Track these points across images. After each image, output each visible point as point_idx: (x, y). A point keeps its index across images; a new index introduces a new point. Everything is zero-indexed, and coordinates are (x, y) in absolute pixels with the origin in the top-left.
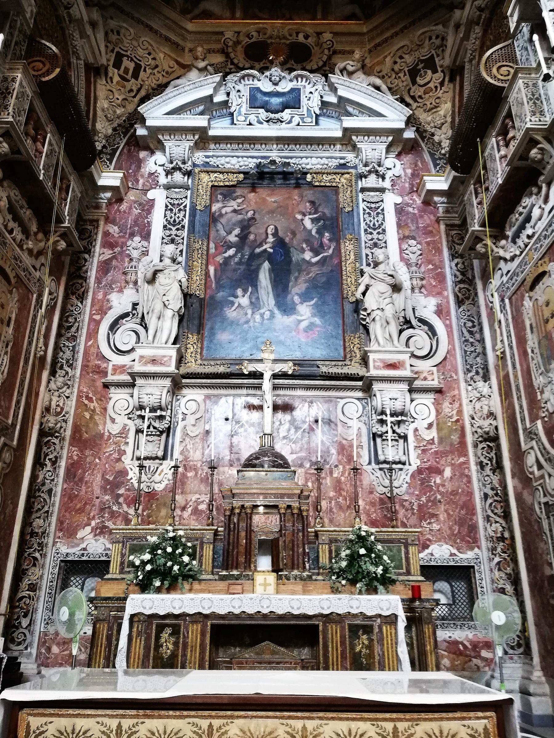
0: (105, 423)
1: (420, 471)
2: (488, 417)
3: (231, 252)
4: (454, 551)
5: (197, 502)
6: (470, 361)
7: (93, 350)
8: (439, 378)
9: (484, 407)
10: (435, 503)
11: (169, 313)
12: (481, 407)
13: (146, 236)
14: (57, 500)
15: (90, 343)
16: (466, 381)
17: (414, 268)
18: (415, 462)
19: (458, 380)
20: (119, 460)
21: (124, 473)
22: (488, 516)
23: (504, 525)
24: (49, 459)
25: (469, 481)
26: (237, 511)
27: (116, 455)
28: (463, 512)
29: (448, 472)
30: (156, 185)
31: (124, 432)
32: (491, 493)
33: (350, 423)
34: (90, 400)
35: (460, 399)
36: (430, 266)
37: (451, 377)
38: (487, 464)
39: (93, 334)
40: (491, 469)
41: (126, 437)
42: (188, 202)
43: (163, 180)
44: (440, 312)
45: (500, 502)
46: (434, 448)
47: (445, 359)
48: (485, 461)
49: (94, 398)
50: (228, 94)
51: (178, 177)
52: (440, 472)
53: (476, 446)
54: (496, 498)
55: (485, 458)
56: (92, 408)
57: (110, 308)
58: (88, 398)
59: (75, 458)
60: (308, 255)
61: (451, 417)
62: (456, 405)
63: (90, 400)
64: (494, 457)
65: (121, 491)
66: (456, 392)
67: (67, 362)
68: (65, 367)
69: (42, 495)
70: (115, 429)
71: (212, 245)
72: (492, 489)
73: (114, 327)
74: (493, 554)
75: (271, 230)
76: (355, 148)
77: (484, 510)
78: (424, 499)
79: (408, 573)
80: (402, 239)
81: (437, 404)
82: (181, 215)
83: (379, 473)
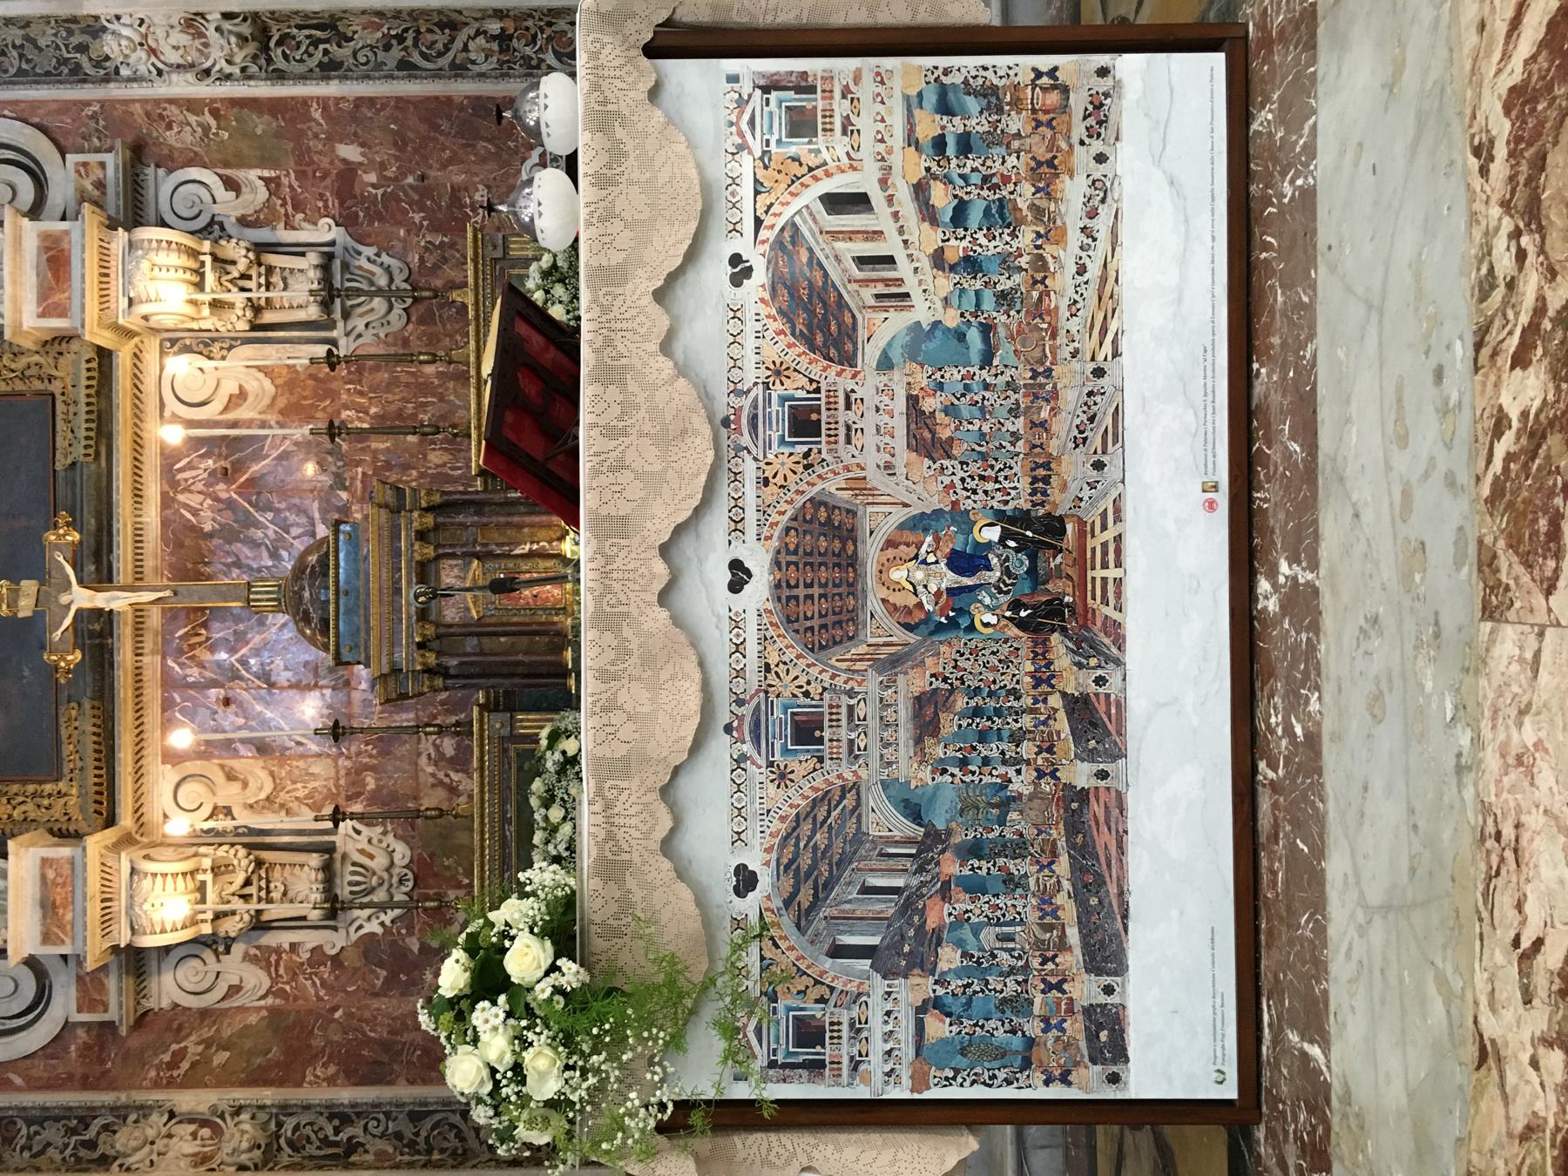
0: (242, 1009)
1: (346, 221)
2: (201, 35)
5: (439, 759)
6: (47, 63)
7: (39, 1068)
8: (98, 151)
9: (173, 40)
10: (425, 190)
12: (176, 48)
15: (18, 1081)
16: (106, 80)
18: (326, 231)
19: (102, 103)
20: (336, 960)
22: (453, 65)
23: (472, 32)
24: (336, 1134)
25: (371, 101)
26: (431, 659)
27: (325, 971)
28: (445, 126)
31: (265, 959)
32: (396, 53)
33: (230, 387)
34: (179, 1056)
35: (157, 102)
37: (94, 117)
38: (326, 52)
40: (339, 46)
41: (278, 951)
45: (418, 32)
46: (289, 179)
48: (319, 55)
49: (175, 1047)
52: (349, 172)
53: (280, 76)
54: (409, 42)
55: (311, 55)
56: (200, 1048)
58: (173, 1065)
59: (332, 1069)
61: (206, 129)
62: (173, 111)
63: (179, 1056)
64: (307, 32)
66: (137, 109)
67: (73, 1131)
68: (90, 1134)
69: (423, 1134)
70: (256, 980)
72: (387, 48)
74: (538, 67)
77: (437, 75)
78: (417, 217)
81: (171, 162)
83: (358, 323)
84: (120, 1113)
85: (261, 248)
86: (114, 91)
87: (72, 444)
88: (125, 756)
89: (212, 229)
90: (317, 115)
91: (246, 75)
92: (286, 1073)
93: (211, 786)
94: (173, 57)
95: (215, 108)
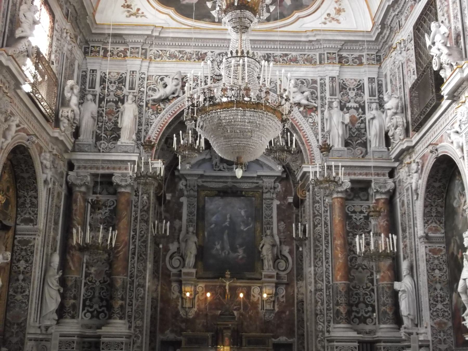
1: (278, 312)
3: (213, 226)
4: (287, 339)
11: (192, 255)
13: (180, 219)
14: (158, 322)
17: (282, 234)
18: (277, 309)
20: (177, 307)
21: (178, 312)
29: (287, 313)
30: (183, 195)
31: (177, 298)
33: (255, 295)
36: (289, 233)
39: (164, 260)
41: (178, 299)
42: (196, 204)
43: (186, 193)
44: (291, 252)
46: (284, 304)
47: (290, 271)
50: (212, 156)
51: (192, 192)
52: (284, 312)
53: (297, 303)
57: (169, 250)
60: (242, 228)
65: (178, 318)
70: (175, 297)
71: (206, 223)
73: (171, 258)
75: (228, 216)
76: (262, 180)
77: (298, 325)
79: (268, 346)
80: (279, 221)
81: (286, 289)
82: (193, 209)
84: (158, 278)
85: (274, 302)
86: (295, 282)
87: (248, 275)
88: (207, 280)
89: (276, 294)
90: (293, 308)
91: (297, 299)
92: (162, 300)
93: (202, 291)
94: (300, 290)
95: (293, 295)
